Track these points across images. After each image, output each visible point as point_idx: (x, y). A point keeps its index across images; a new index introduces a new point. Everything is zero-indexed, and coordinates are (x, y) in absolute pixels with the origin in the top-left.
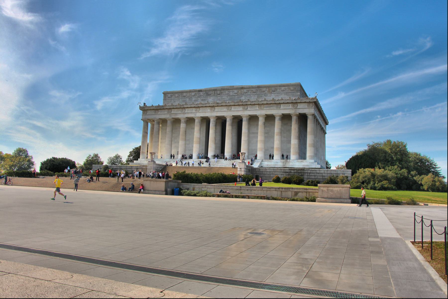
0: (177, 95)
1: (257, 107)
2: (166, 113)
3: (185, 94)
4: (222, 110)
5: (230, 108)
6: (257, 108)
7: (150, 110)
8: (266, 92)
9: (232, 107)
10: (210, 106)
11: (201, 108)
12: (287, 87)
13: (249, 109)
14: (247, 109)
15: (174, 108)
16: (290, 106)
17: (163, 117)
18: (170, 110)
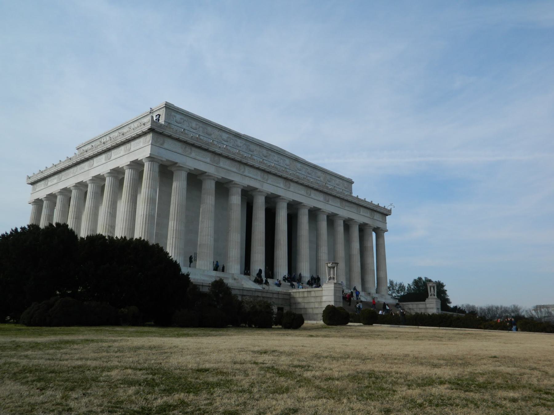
0: (194, 124)
1: (338, 203)
2: (208, 160)
3: (210, 129)
4: (300, 192)
5: (309, 191)
6: (339, 205)
7: (178, 140)
8: (322, 179)
9: (313, 191)
10: (286, 179)
11: (270, 176)
12: (341, 181)
13: (330, 202)
14: (328, 201)
15: (227, 158)
16: (368, 213)
17: (202, 167)
18: (217, 158)
